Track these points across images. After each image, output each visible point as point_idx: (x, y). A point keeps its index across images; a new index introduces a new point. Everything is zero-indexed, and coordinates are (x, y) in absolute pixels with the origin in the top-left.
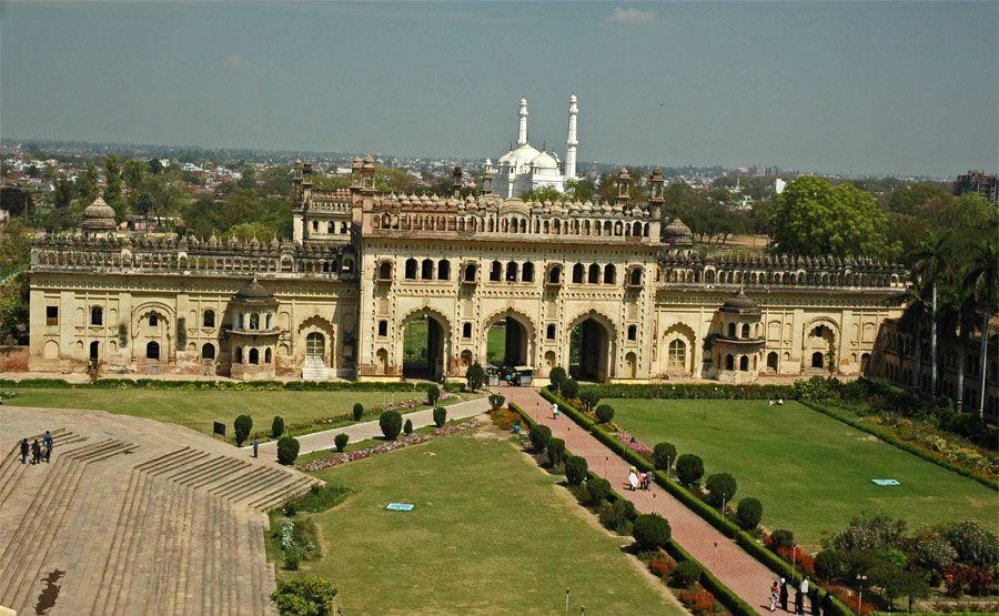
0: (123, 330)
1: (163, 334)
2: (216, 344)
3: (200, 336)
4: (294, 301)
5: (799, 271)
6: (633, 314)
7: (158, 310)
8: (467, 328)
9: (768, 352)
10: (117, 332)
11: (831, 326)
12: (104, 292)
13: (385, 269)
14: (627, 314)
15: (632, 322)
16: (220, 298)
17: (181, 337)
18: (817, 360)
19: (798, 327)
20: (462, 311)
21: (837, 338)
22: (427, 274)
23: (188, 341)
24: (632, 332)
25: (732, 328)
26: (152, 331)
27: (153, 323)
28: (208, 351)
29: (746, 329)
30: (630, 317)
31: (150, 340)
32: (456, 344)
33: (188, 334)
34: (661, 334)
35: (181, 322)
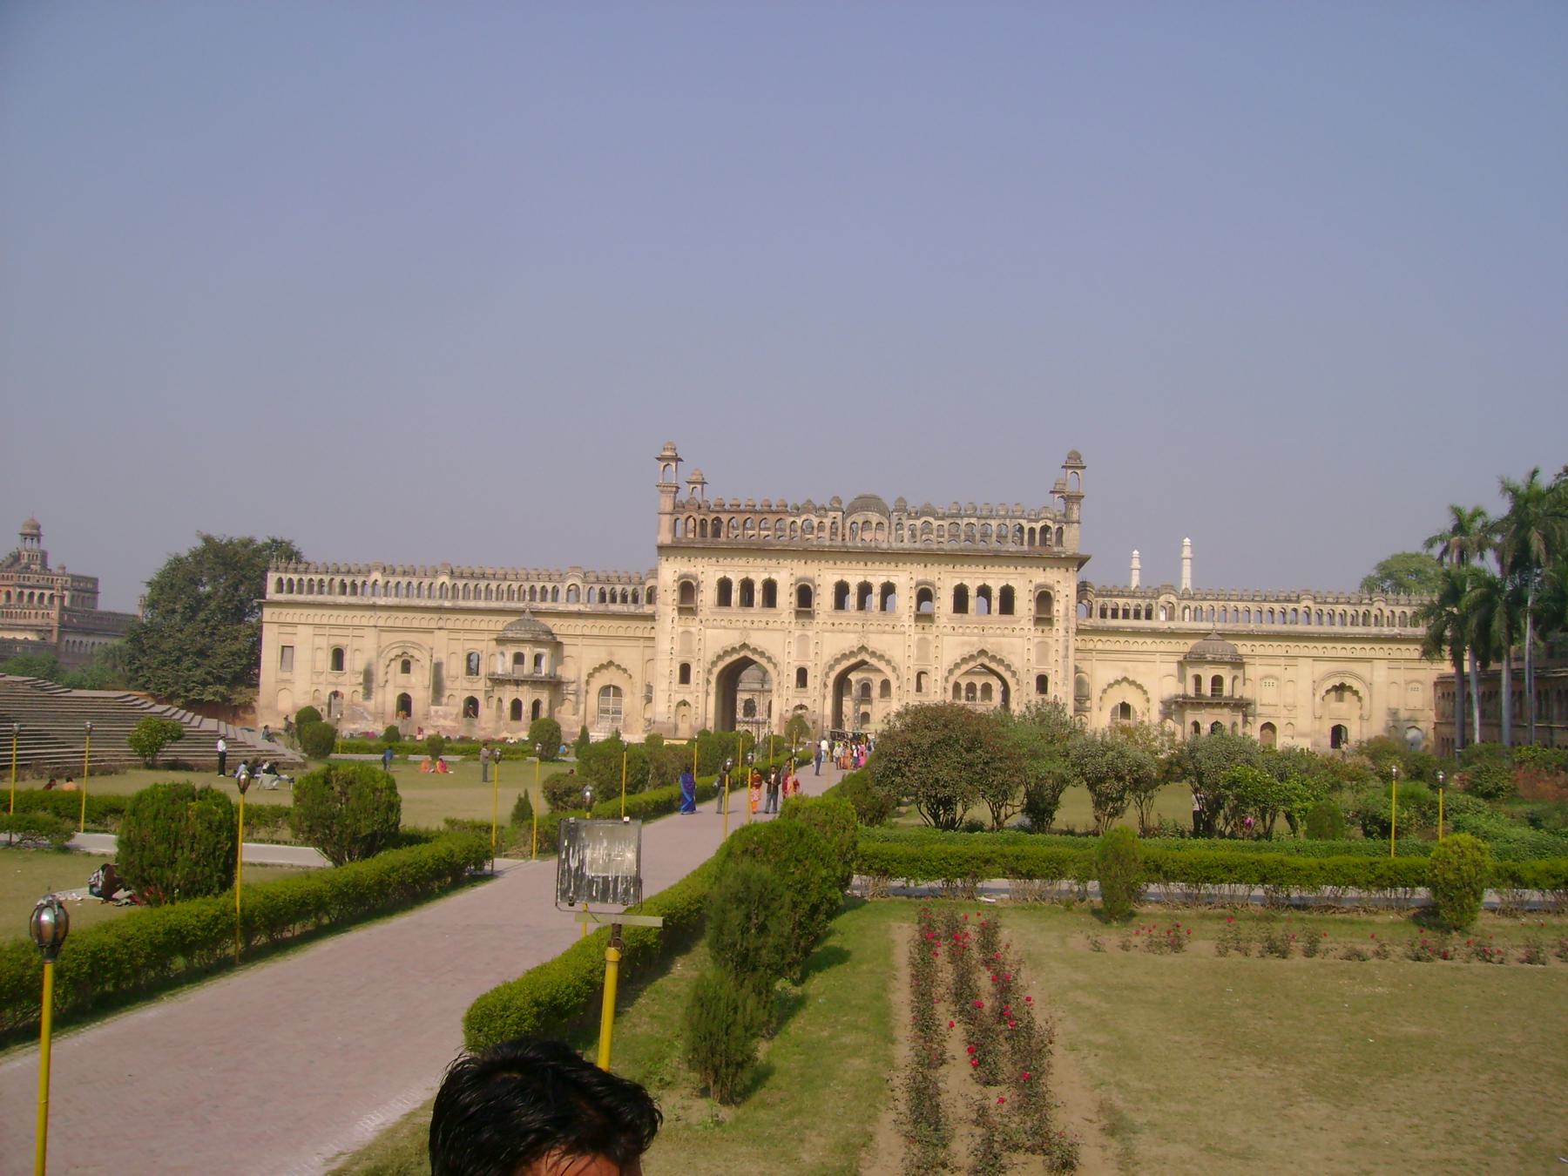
0: (368, 676)
1: (418, 685)
2: (481, 697)
3: (459, 688)
4: (579, 641)
5: (1305, 603)
6: (1043, 654)
7: (411, 652)
8: (802, 675)
9: (1261, 722)
10: (361, 679)
11: (1356, 685)
12: (346, 627)
13: (687, 589)
14: (1033, 657)
15: (1042, 669)
16: (486, 636)
17: (438, 688)
18: (1338, 734)
19: (1305, 686)
20: (794, 649)
21: (1366, 701)
22: (747, 601)
23: (447, 693)
24: (1042, 683)
25: (1198, 679)
26: (402, 678)
27: (406, 667)
28: (472, 706)
29: (1217, 681)
30: (1039, 661)
31: (401, 691)
32: (782, 701)
33: (447, 683)
34: (1096, 694)
35: (438, 668)
